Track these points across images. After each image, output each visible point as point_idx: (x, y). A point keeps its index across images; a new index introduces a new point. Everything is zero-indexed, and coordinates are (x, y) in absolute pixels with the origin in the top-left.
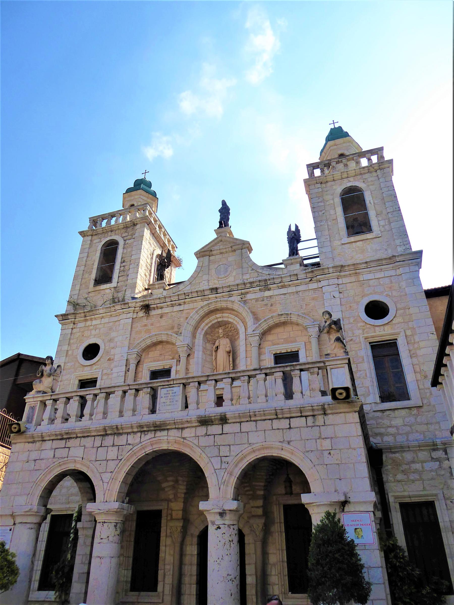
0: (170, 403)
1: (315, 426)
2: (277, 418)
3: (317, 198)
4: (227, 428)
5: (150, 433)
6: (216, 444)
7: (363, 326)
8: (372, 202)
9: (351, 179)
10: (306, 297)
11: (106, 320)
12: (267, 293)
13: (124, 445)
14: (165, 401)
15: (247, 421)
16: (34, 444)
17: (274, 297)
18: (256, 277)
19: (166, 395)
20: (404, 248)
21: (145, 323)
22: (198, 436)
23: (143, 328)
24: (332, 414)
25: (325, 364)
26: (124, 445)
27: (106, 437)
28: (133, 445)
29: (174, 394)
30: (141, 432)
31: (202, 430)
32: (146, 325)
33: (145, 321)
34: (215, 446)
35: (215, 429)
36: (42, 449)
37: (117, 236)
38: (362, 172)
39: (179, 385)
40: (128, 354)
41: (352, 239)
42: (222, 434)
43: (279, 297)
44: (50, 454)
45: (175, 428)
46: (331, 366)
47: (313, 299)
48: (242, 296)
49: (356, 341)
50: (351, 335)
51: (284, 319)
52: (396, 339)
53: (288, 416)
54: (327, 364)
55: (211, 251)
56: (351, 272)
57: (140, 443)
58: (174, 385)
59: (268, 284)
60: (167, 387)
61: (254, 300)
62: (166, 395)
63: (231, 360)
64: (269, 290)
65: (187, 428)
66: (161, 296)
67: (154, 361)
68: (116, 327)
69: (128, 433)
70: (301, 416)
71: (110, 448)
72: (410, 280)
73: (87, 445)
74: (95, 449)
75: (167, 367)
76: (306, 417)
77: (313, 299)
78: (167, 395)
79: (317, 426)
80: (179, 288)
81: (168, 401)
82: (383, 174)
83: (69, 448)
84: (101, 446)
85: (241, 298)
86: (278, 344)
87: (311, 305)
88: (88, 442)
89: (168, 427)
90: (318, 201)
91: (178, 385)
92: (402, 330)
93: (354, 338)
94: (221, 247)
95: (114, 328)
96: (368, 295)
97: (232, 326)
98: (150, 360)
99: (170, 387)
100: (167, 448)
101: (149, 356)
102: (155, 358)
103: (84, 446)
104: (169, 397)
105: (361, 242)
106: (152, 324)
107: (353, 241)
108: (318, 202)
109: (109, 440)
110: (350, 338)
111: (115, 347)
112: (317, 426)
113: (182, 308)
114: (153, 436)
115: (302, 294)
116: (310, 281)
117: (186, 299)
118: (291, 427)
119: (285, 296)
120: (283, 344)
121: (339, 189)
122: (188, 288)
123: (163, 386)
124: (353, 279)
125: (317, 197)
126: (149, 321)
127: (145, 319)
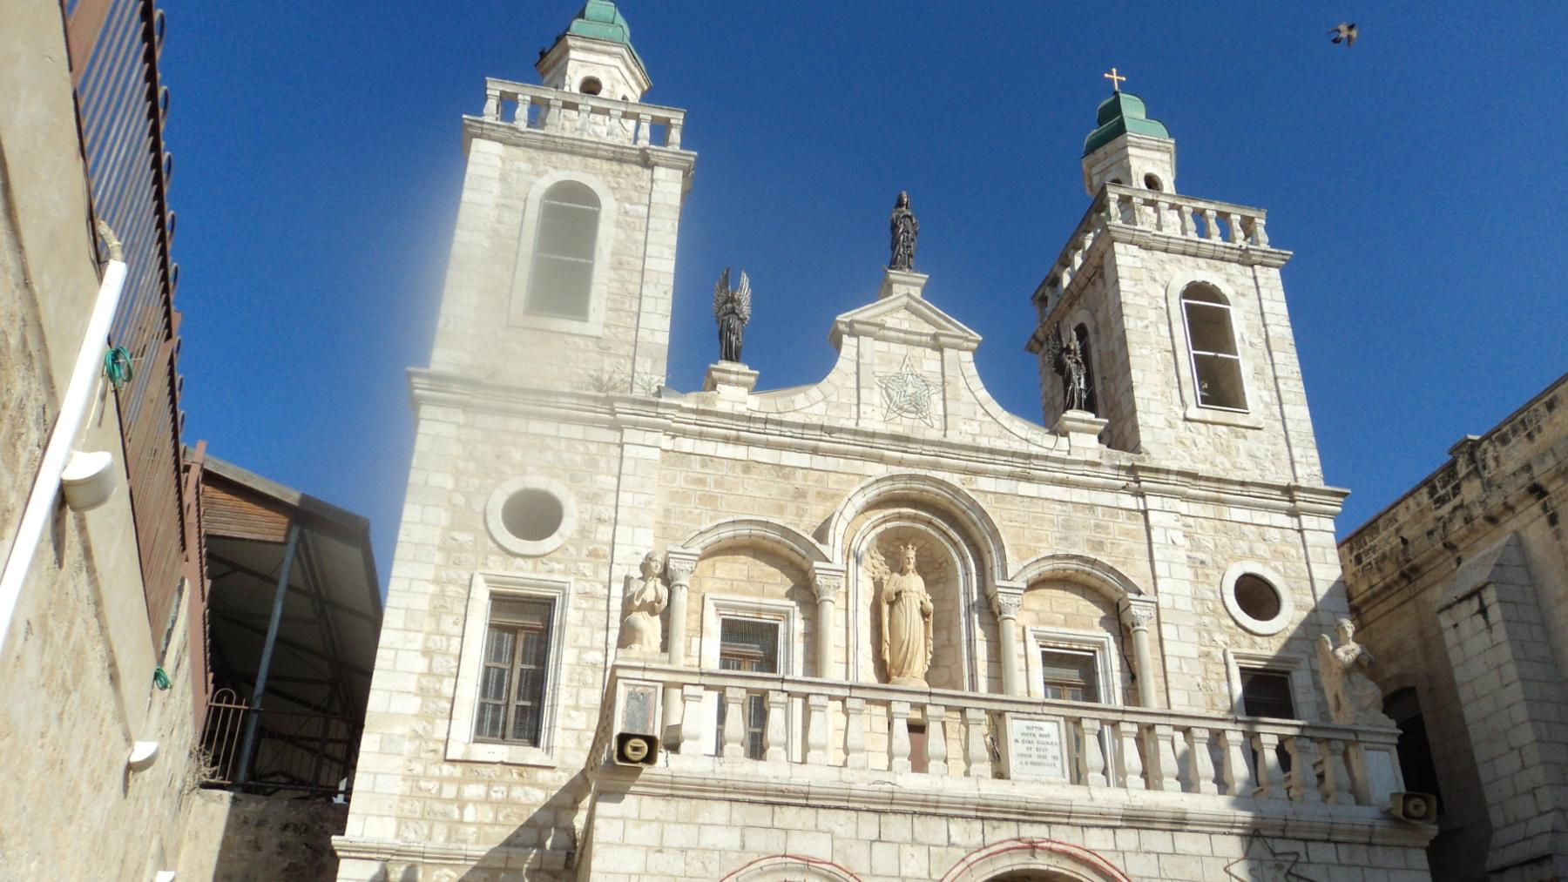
0: (1039, 760)
1: (1353, 865)
2: (1283, 838)
3: (1133, 283)
4: (1185, 841)
5: (1005, 823)
6: (1163, 876)
7: (1232, 628)
8: (1246, 337)
9: (1201, 262)
10: (1111, 524)
11: (577, 431)
12: (1025, 488)
13: (941, 846)
14: (1025, 752)
15: (1225, 833)
16: (674, 802)
17: (1040, 502)
18: (996, 437)
19: (1026, 738)
20: (1308, 471)
21: (700, 476)
22: (1123, 852)
23: (694, 487)
24: (1384, 846)
25: (1356, 735)
26: (941, 846)
27: (891, 818)
28: (965, 848)
29: (1045, 740)
30: (982, 819)
31: (1128, 838)
32: (701, 481)
33: (699, 469)
34: (1162, 879)
35: (1158, 840)
36: (700, 820)
37: (593, 178)
38: (1226, 256)
39: (1057, 718)
40: (670, 555)
41: (1210, 414)
42: (1174, 853)
43: (1052, 506)
44: (730, 839)
45: (1068, 824)
46: (1367, 745)
47: (1127, 533)
48: (963, 476)
49: (1217, 661)
50: (1207, 643)
51: (1076, 566)
52: (1288, 673)
53: (1305, 835)
54: (1361, 737)
55: (882, 327)
56: (1211, 494)
57: (985, 848)
58: (1044, 717)
59: (1032, 466)
60: (1026, 716)
61: (992, 496)
62: (1026, 738)
63: (931, 635)
64: (1029, 479)
65: (1092, 826)
66: (740, 409)
67: (733, 590)
68: (608, 463)
69: (947, 816)
70: (1328, 841)
71: (907, 849)
72: (1319, 549)
73: (838, 830)
74: (864, 848)
75: (767, 619)
76: (1336, 842)
77: (1127, 533)
78: (1030, 738)
79: (1357, 866)
80: (793, 402)
81: (1034, 753)
82: (1267, 279)
83: (786, 830)
84: (879, 840)
85: (961, 480)
86: (1053, 624)
87: (1123, 547)
88: (841, 823)
89: (1051, 819)
90: (1135, 290)
91: (1053, 718)
92: (1305, 657)
93: (1213, 650)
94: (905, 326)
95: (602, 464)
96: (1242, 558)
97: (928, 545)
98: (718, 585)
99: (1032, 720)
100: (1045, 868)
101: (717, 572)
102: (735, 583)
103: (832, 833)
104: (1035, 746)
105: (1224, 429)
106: (718, 484)
107: (1210, 418)
108: (1136, 295)
109: (897, 827)
110: (1205, 649)
111: (613, 521)
112: (1357, 866)
113: (803, 460)
114: (1015, 835)
115: (1103, 515)
116: (1124, 488)
117: (820, 440)
118: (1312, 859)
119: (1064, 508)
120: (1062, 626)
121: (1179, 284)
122: (820, 409)
123: (1017, 712)
124: (1209, 510)
125: (1131, 278)
126: (708, 471)
127: (698, 465)
